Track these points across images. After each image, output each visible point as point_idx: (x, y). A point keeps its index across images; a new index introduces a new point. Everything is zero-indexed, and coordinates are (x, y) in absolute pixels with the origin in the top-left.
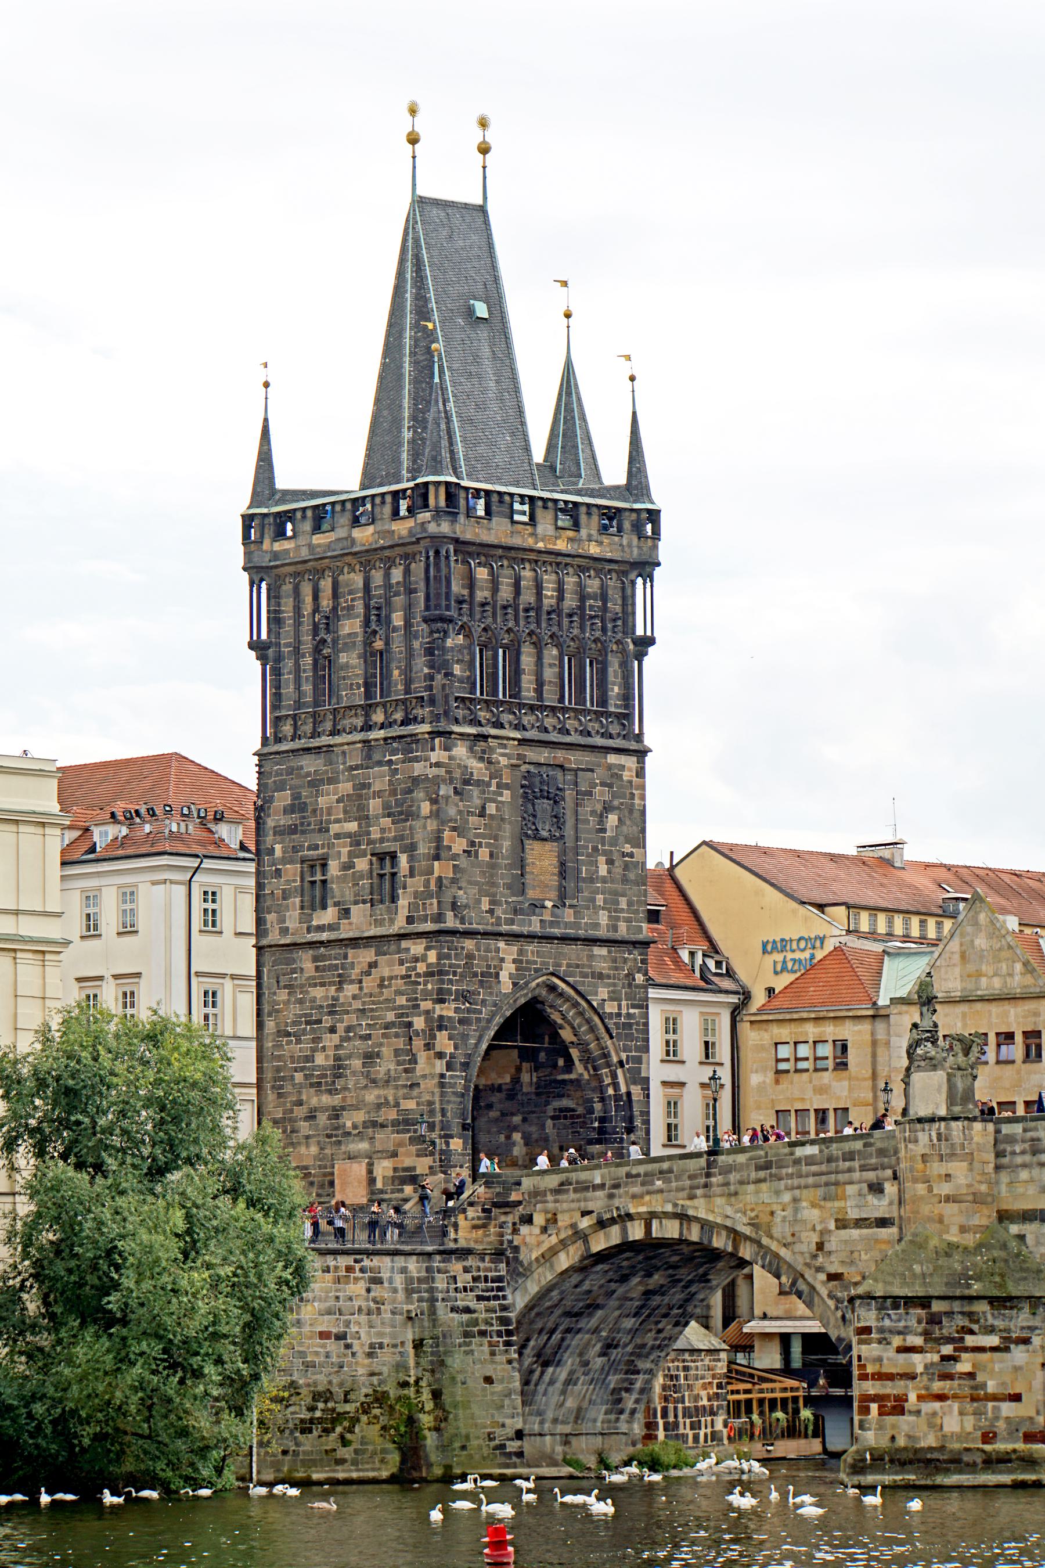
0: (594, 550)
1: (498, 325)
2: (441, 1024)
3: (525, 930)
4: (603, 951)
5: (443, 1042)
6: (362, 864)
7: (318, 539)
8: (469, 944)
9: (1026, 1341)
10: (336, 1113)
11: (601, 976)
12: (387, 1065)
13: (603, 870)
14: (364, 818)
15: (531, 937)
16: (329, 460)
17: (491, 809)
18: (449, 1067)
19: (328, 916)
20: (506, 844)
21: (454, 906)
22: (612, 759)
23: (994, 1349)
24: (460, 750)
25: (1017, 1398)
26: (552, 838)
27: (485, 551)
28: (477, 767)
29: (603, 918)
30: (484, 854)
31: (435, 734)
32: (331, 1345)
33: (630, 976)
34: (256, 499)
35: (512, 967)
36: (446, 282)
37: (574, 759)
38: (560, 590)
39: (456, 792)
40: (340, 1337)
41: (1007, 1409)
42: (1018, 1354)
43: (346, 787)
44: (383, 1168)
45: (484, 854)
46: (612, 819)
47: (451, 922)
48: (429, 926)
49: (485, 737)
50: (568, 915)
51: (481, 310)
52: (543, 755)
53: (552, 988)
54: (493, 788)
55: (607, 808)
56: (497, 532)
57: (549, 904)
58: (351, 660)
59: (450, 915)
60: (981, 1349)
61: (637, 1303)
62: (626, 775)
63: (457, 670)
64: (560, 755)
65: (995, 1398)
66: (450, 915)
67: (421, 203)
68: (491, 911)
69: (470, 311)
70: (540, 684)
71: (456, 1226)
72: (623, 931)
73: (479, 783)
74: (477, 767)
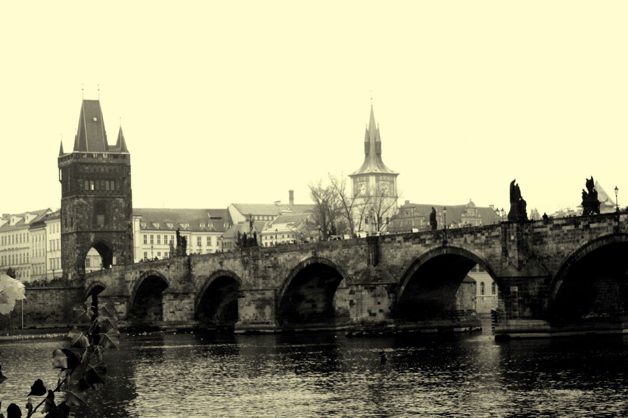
0: (111, 162)
1: (100, 122)
2: (77, 248)
3: (96, 230)
4: (115, 233)
5: (78, 251)
6: (70, 220)
7: (65, 162)
8: (84, 234)
9: (124, 303)
10: (69, 263)
11: (114, 238)
12: (73, 255)
13: (115, 219)
14: (70, 212)
15: (98, 232)
16: (69, 149)
17: (88, 209)
18: (79, 255)
19: (67, 229)
20: (92, 216)
21: (80, 227)
22: (117, 199)
23: (119, 305)
24: (81, 200)
25: (122, 313)
26: (103, 214)
27: (87, 164)
28: (85, 202)
29: (115, 227)
30: (87, 218)
31: (76, 197)
32: (42, 305)
33: (121, 238)
34: (60, 155)
35: (93, 237)
36: (91, 114)
37: (107, 200)
38: (105, 169)
39: (81, 207)
40: (44, 304)
41: (120, 315)
42: (123, 306)
43: (68, 206)
44: (73, 273)
45: (87, 218)
46: (117, 210)
47: (79, 230)
48: (75, 231)
49: (87, 197)
50: (107, 227)
51: (95, 119)
52: (100, 199)
53: (103, 240)
54: (89, 206)
55: (116, 208)
56: (90, 160)
57: (102, 226)
58: (69, 183)
59: (79, 229)
60: (117, 305)
61: (163, 292)
62: (120, 202)
63: (81, 185)
64: (105, 199)
65: (119, 313)
66: (79, 229)
67: (85, 101)
68: (89, 228)
69: (93, 120)
70: (100, 186)
71: (72, 284)
72: (119, 229)
73: (85, 205)
74: (85, 202)
